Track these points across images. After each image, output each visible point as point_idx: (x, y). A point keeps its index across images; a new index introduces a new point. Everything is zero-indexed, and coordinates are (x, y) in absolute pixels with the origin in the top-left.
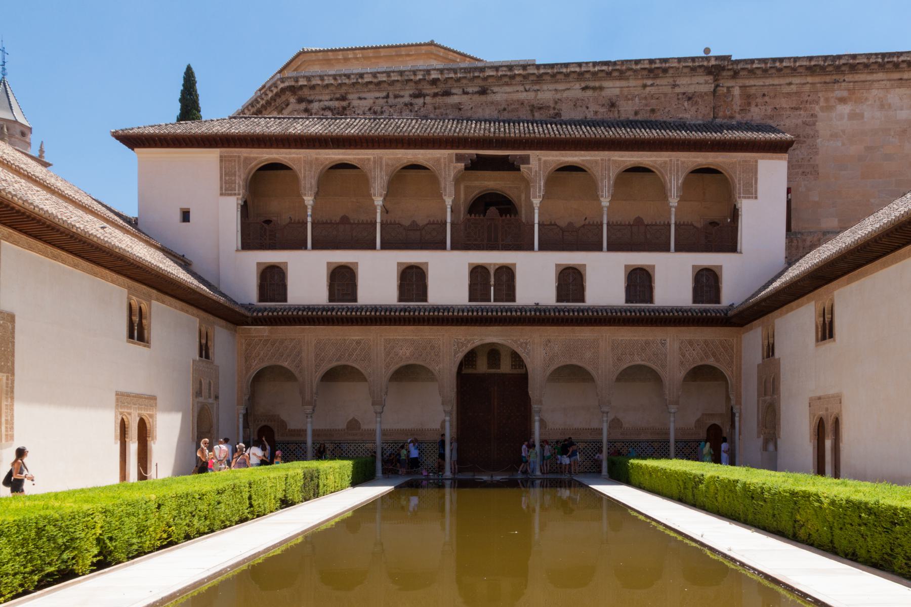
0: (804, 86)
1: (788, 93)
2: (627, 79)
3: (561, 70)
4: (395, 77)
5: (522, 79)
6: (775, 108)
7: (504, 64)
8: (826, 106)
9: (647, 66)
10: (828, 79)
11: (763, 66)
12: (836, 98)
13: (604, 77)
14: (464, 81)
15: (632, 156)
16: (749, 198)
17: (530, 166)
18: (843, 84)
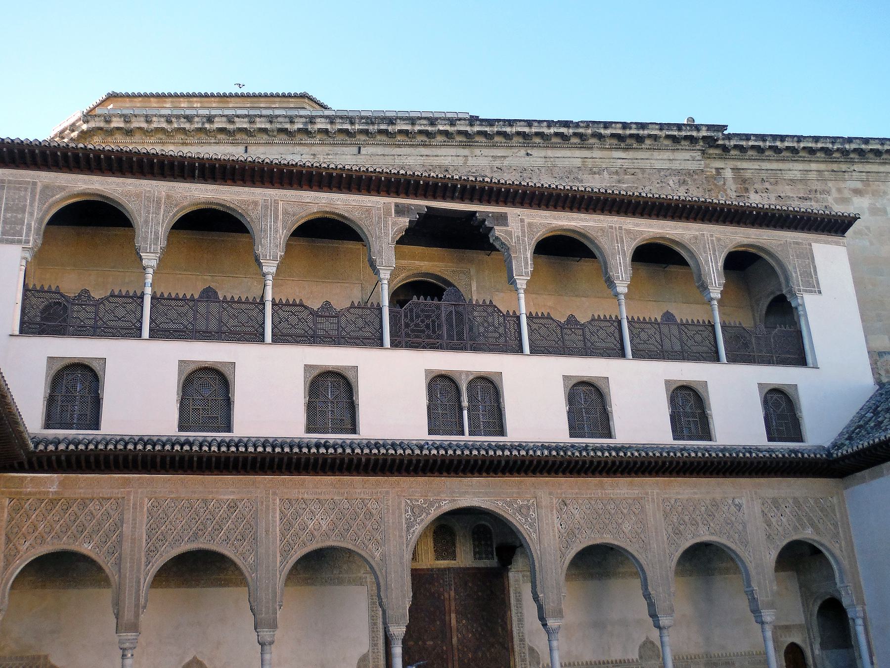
0: (809, 173)
1: (791, 180)
2: (590, 148)
3: (504, 129)
4: (261, 124)
5: (444, 138)
6: (780, 196)
7: (424, 115)
8: (840, 198)
9: (620, 132)
10: (835, 167)
11: (761, 144)
12: (850, 189)
13: (559, 143)
14: (363, 137)
15: (651, 226)
16: (811, 292)
17: (509, 229)
18: (854, 174)
